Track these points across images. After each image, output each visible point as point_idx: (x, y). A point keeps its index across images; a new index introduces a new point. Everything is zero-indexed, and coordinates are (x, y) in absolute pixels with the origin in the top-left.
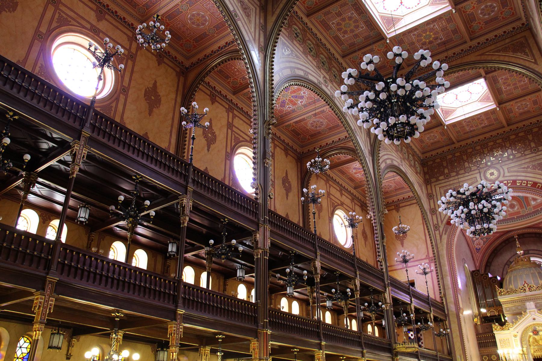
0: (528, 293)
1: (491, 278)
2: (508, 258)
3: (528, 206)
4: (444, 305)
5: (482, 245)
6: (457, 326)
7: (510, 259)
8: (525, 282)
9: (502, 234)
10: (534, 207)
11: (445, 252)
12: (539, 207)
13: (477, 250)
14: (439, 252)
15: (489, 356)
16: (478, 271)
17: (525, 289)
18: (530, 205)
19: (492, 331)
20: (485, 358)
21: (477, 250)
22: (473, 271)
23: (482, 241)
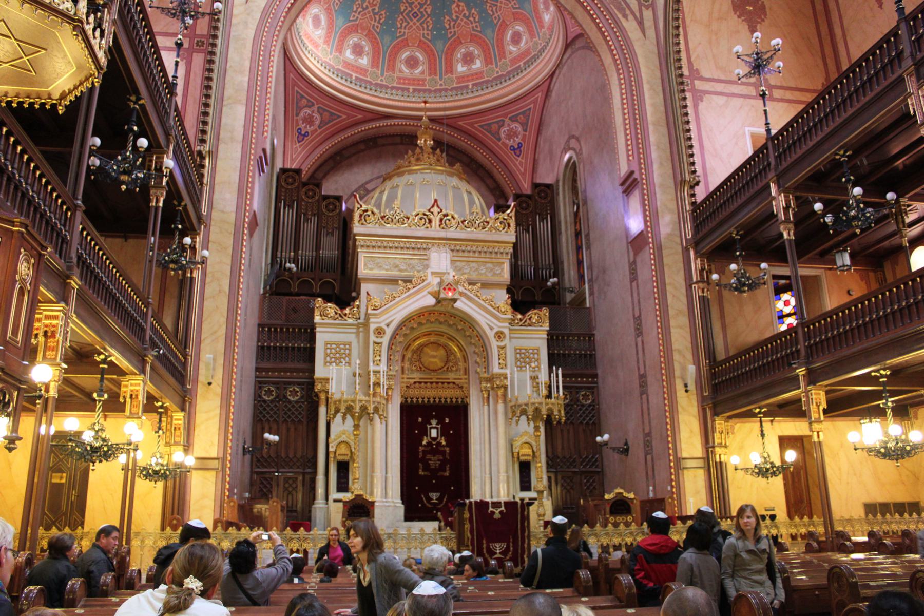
0: (435, 230)
1: (326, 197)
2: (364, 181)
3: (446, 72)
4: (202, 184)
5: (316, 127)
6: (229, 262)
7: (367, 183)
8: (436, 201)
9: (369, 116)
10: (462, 78)
11: (251, 33)
12: (473, 80)
13: (300, 133)
14: (233, 29)
15: (281, 386)
16: (298, 172)
17: (430, 221)
18: (451, 72)
19: (313, 318)
20: (269, 392)
21: (300, 133)
22: (284, 171)
23: (316, 115)
